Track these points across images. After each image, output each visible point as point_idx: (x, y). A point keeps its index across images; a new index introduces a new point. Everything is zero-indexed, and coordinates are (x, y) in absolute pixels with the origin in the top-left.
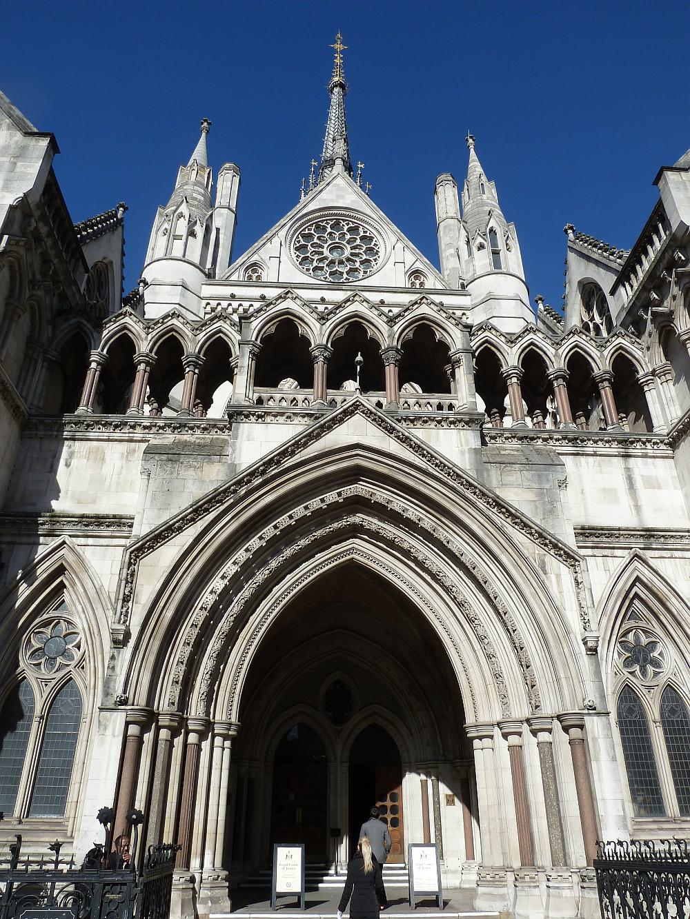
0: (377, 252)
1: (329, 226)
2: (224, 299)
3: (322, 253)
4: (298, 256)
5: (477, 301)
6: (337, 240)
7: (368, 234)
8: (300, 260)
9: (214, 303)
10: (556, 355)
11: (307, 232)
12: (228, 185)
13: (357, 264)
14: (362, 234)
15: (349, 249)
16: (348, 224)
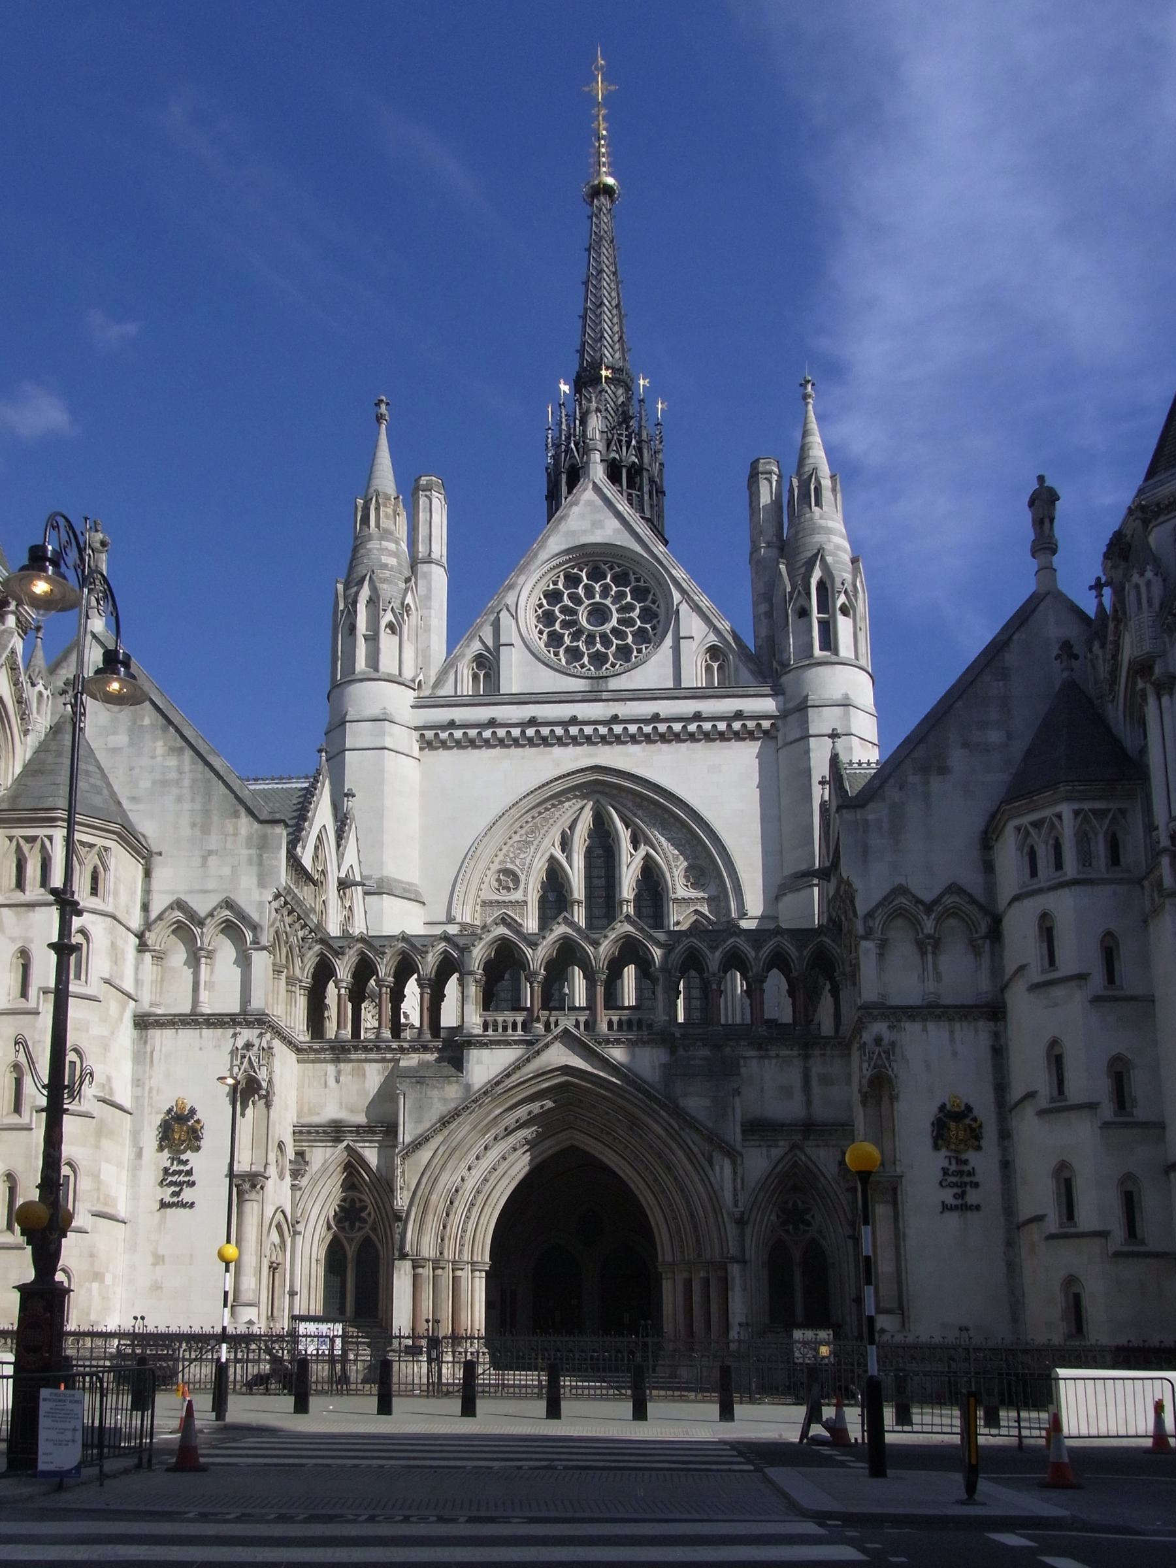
0: (656, 616)
1: (584, 575)
2: (443, 728)
3: (575, 623)
4: (541, 632)
5: (791, 705)
6: (597, 598)
7: (642, 584)
8: (545, 636)
9: (429, 734)
10: (756, 958)
11: (552, 586)
12: (436, 514)
13: (630, 640)
14: (633, 584)
15: (614, 612)
16: (611, 569)
